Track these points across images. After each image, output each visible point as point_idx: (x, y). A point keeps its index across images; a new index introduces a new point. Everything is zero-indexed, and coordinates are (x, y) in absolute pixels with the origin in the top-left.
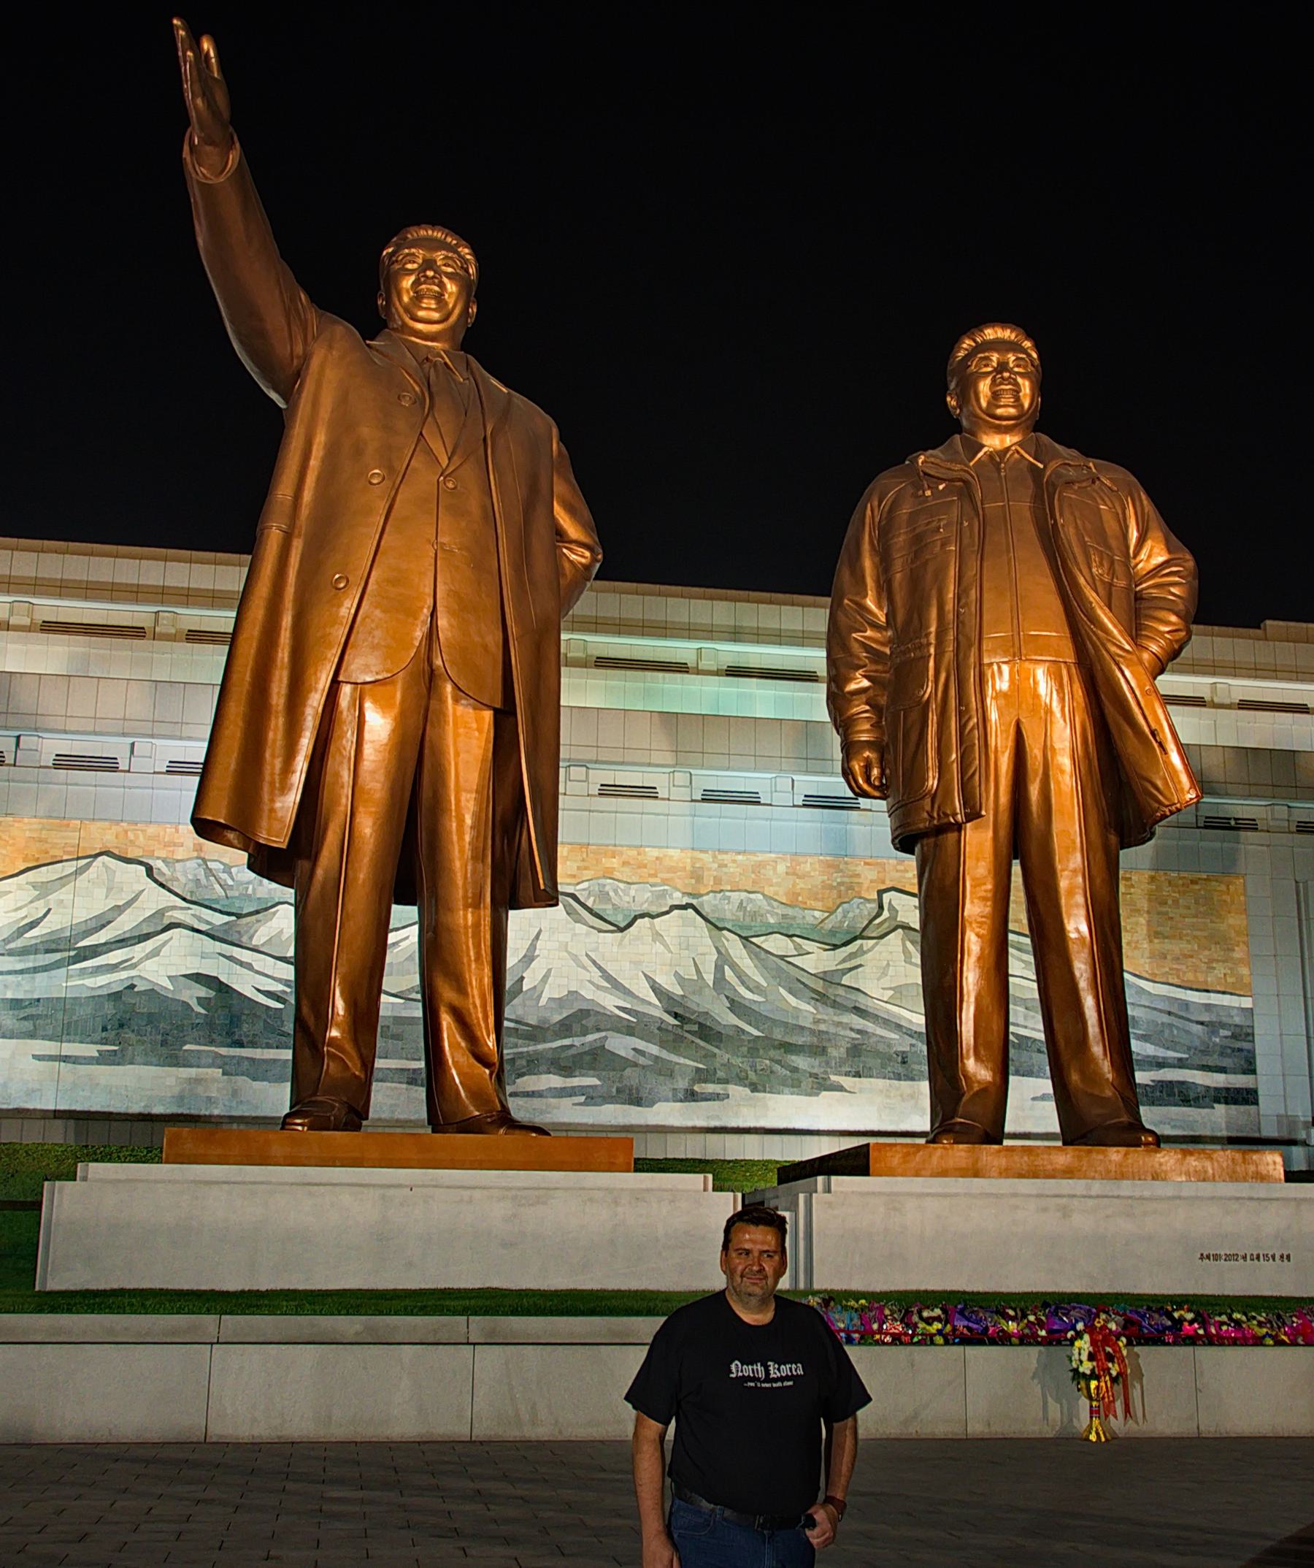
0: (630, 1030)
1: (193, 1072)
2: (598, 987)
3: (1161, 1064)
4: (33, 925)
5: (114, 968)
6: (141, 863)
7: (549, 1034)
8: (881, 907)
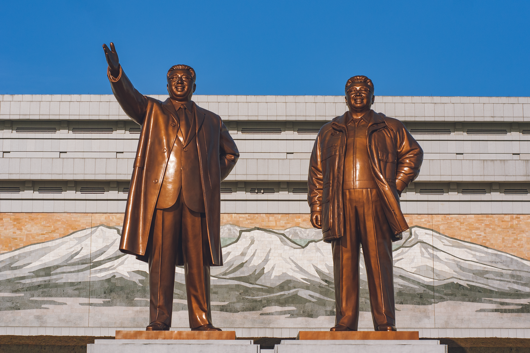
0: (307, 288)
2: (294, 271)
4: (77, 254)
6: (115, 229)
7: (275, 290)
8: (411, 234)
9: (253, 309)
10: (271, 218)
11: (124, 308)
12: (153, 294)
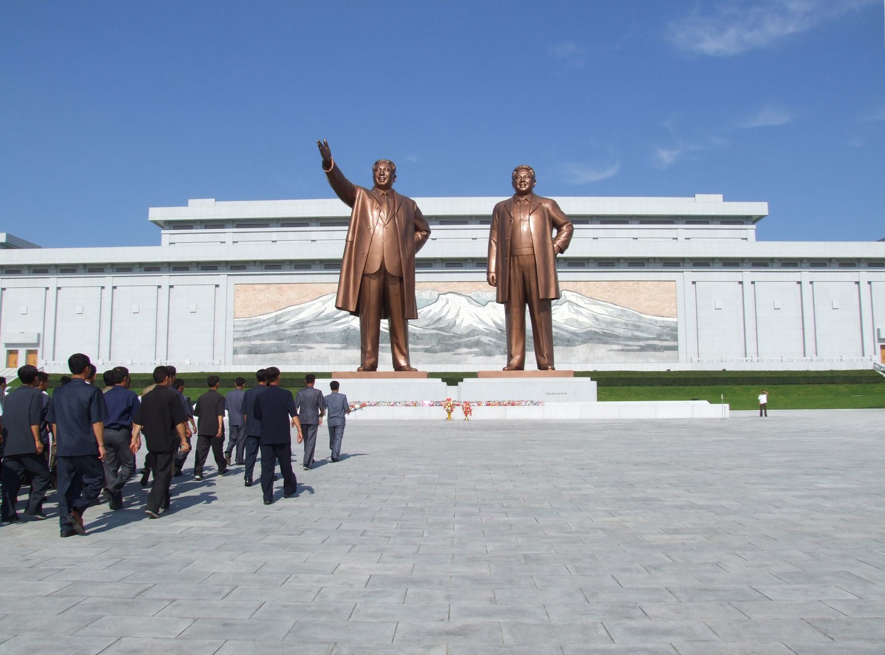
0: (487, 335)
3: (648, 339)
5: (344, 323)
9: (448, 351)
10: (461, 284)
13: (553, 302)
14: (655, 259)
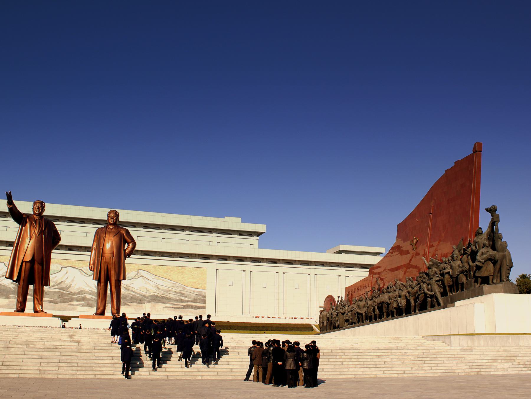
0: (90, 294)
1: (11, 300)
3: (188, 301)
9: (65, 302)
10: (77, 262)
11: (4, 299)
12: (18, 296)
13: (122, 282)
14: (195, 254)
